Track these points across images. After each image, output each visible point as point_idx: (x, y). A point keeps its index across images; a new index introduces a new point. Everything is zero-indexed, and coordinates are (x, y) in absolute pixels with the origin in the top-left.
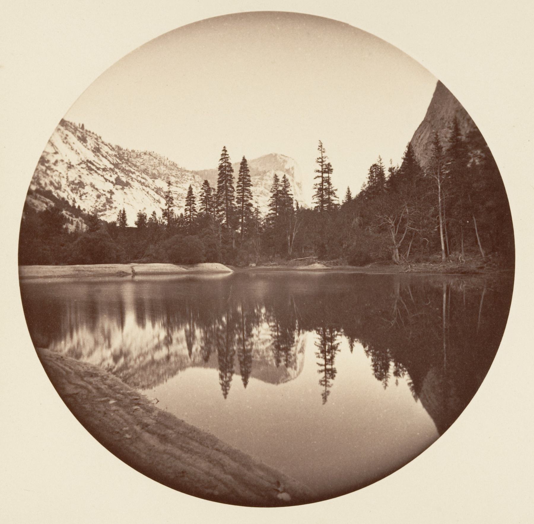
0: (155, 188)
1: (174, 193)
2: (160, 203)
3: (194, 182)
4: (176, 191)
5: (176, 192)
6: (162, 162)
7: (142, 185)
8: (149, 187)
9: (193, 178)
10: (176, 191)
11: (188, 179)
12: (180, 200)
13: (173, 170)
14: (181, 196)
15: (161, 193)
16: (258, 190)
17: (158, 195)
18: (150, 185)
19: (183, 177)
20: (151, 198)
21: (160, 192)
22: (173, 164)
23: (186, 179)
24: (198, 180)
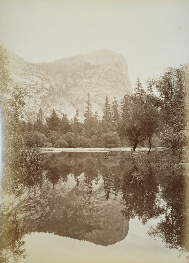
9: (38, 71)
11: (34, 72)
19: (30, 69)
23: (33, 72)
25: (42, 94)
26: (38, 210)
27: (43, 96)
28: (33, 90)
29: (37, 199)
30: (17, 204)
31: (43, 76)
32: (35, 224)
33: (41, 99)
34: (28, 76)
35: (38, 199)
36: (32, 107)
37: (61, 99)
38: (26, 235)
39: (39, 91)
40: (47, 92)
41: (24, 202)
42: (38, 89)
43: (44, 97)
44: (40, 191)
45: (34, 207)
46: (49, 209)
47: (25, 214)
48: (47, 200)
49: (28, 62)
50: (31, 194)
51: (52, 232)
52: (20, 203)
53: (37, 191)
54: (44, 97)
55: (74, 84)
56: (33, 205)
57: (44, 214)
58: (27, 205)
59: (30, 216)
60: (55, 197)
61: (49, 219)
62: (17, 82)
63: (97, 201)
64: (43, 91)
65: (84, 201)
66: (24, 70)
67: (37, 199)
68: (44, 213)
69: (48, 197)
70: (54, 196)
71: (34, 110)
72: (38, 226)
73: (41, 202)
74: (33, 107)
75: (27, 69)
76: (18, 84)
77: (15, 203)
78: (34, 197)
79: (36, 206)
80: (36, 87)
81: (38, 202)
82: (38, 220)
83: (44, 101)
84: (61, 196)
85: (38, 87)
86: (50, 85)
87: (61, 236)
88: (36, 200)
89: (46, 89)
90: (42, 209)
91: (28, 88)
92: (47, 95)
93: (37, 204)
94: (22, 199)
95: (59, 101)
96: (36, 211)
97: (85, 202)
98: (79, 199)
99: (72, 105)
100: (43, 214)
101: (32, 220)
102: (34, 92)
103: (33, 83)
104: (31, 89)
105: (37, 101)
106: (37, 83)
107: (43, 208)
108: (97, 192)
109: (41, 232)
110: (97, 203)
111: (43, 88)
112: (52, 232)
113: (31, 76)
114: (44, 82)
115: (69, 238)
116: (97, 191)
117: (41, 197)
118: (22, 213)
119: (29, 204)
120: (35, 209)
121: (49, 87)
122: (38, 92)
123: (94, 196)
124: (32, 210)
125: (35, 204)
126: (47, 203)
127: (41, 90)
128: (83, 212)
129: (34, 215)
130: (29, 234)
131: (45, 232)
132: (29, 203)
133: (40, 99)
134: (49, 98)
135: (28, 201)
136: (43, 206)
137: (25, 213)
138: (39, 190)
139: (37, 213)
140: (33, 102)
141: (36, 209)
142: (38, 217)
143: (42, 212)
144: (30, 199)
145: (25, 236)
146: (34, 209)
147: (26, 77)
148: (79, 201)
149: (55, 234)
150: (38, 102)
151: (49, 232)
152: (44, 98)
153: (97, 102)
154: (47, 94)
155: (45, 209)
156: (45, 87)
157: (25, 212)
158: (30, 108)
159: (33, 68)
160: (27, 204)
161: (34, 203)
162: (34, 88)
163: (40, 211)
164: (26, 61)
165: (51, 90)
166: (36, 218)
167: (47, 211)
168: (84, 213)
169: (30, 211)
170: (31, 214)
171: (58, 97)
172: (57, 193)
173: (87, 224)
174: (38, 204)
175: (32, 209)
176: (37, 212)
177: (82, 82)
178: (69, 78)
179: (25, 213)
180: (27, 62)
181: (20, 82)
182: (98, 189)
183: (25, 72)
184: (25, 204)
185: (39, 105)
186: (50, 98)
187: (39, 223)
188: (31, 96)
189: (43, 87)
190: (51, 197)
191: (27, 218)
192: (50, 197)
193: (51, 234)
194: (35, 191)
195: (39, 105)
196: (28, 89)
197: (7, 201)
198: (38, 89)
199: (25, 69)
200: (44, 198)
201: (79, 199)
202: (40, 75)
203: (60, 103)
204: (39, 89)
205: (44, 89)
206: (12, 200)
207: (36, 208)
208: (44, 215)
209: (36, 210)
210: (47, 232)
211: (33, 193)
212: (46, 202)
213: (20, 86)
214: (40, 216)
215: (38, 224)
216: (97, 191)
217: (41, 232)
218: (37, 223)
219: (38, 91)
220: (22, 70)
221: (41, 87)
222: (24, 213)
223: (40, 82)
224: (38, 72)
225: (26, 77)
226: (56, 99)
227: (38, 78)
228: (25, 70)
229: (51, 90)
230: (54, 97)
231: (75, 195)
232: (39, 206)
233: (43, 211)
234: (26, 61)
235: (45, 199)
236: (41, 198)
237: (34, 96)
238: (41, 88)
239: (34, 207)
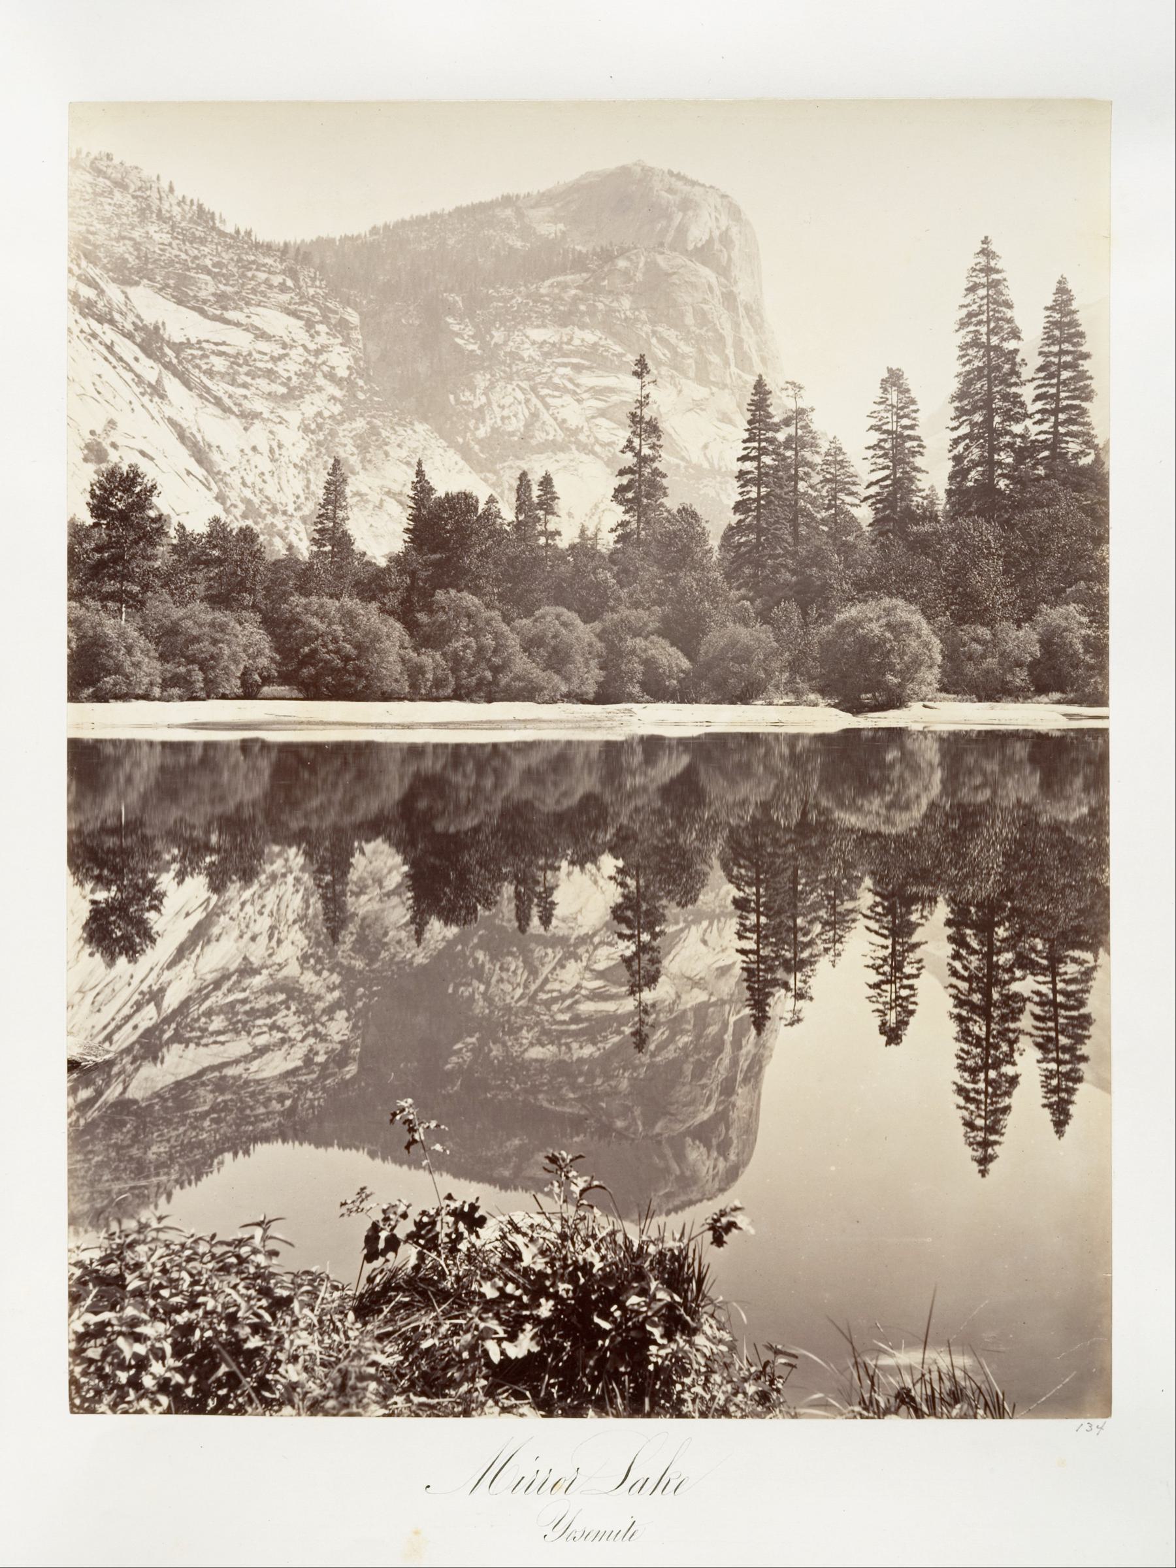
0: (137, 328)
1: (213, 352)
2: (162, 397)
3: (297, 299)
4: (224, 343)
5: (223, 348)
6: (149, 206)
7: (85, 316)
8: (112, 322)
9: (290, 283)
10: (224, 343)
11: (271, 287)
12: (245, 385)
13: (203, 242)
14: (246, 363)
15: (167, 350)
16: (576, 342)
17: (151, 362)
18: (117, 316)
19: (249, 274)
20: (129, 376)
21: (161, 349)
22: (200, 217)
23: (263, 288)
24: (311, 291)
25: (312, 404)
26: (286, 1032)
27: (320, 414)
28: (263, 383)
29: (285, 972)
30: (182, 996)
31: (315, 310)
32: (274, 1102)
33: (306, 429)
34: (235, 309)
35: (293, 969)
36: (263, 474)
37: (410, 432)
38: (228, 1156)
39: (295, 388)
40: (338, 393)
41: (217, 985)
42: (289, 379)
43: (320, 420)
44: (301, 929)
45: (270, 1011)
46: (345, 1025)
47: (222, 1048)
48: (336, 979)
49: (238, 232)
50: (253, 946)
51: (357, 1143)
52: (199, 990)
53: (283, 927)
54: (320, 420)
55: (479, 352)
56: (261, 1004)
57: (322, 1052)
58: (232, 1005)
59: (247, 1058)
60: (377, 965)
61: (348, 1077)
62: (182, 344)
63: (598, 983)
64: (320, 389)
65: (526, 987)
66: (214, 276)
67: (285, 972)
68: (321, 1047)
69: (339, 964)
70: (372, 958)
71: (271, 490)
72: (291, 1111)
73: (306, 991)
74: (267, 477)
75: (235, 270)
76: (189, 351)
77: (168, 993)
78: (269, 962)
79: (279, 1010)
80: (280, 368)
81: (291, 991)
82: (288, 1083)
83: (319, 443)
84: (409, 956)
85: (290, 368)
86: (354, 357)
87: (405, 1167)
88: (280, 976)
89: (331, 376)
90: (311, 1028)
91: (239, 373)
92: (337, 409)
93: (281, 997)
94: (211, 972)
95: (399, 446)
96: (280, 1035)
97: (533, 987)
99: (468, 468)
100: (317, 1053)
101: (257, 1082)
102: (269, 394)
103: (263, 346)
104: (253, 379)
105: (287, 443)
106: (284, 346)
107: (314, 1021)
108: (596, 940)
109: (301, 1144)
110: (595, 996)
111: (319, 374)
112: (357, 1143)
113: (253, 309)
114: (323, 339)
115: (444, 1174)
116: (594, 934)
117: (304, 958)
118: (206, 1045)
119: (241, 996)
120: (273, 1027)
121: (349, 368)
122: (293, 395)
123: (578, 958)
124: (256, 1031)
125: (273, 1000)
126: (336, 994)
127: (305, 383)
128: (521, 1045)
129: (267, 1057)
130: (240, 1154)
131: (321, 1142)
132: (244, 990)
133: (301, 433)
134: (346, 425)
135: (239, 982)
136: (313, 1011)
137: (223, 1043)
138: (296, 927)
139: (286, 1046)
140: (264, 448)
141: (279, 1023)
142: (290, 1065)
143: (311, 1041)
144: (247, 970)
145: (221, 1163)
146: (265, 1025)
147: (231, 315)
148: (501, 986)
149: (372, 1155)
150: (291, 447)
151: (343, 1146)
152: (320, 427)
153: (597, 448)
154: (338, 405)
155: (323, 1024)
156: (325, 368)
157: (221, 1038)
158: (249, 481)
159: (264, 265)
160: (230, 998)
161: (269, 991)
162: (270, 374)
163: (299, 1037)
164: (229, 229)
165: (361, 383)
166: (277, 1072)
167: (337, 1038)
168: (526, 1050)
169: (249, 1033)
170: (250, 1050)
171: (395, 420)
172: (386, 944)
173: (541, 1106)
174: (290, 997)
175: (260, 1022)
176: (283, 1041)
177: (523, 343)
178: (450, 320)
179: (223, 1043)
180: (232, 237)
181: (199, 342)
182: (598, 925)
183: (222, 287)
184: (225, 995)
185: (295, 465)
186: (354, 425)
187: (292, 1096)
188: (257, 415)
189: (314, 366)
190: (359, 964)
191: (230, 1072)
192: (353, 962)
193: (351, 1154)
194: (272, 928)
195: (295, 465)
196: (240, 381)
197: (132, 977)
198: (289, 379)
199: (224, 271)
200: (319, 967)
201: (504, 975)
202: (301, 304)
203: (404, 453)
204: (294, 378)
205: (320, 380)
206: (159, 976)
207: (279, 1019)
208: (321, 1059)
209: (279, 1029)
210: (332, 1145)
211: (263, 940)
212: (331, 989)
213: (198, 361)
214: (299, 1063)
215: (288, 1103)
216: (594, 934)
217: (301, 1144)
218: (281, 1098)
219: (291, 390)
220: (208, 278)
221: (304, 369)
222: (215, 1042)
223: (301, 342)
224: (290, 288)
225: (231, 315)
226: (384, 433)
227: (292, 321)
228: (223, 275)
229: (361, 383)
230: (377, 422)
231: (480, 955)
232: (293, 1008)
233: (316, 1034)
234: (228, 231)
235: (325, 973)
236: (308, 969)
237: (272, 417)
238: (304, 375)
239: (270, 1011)
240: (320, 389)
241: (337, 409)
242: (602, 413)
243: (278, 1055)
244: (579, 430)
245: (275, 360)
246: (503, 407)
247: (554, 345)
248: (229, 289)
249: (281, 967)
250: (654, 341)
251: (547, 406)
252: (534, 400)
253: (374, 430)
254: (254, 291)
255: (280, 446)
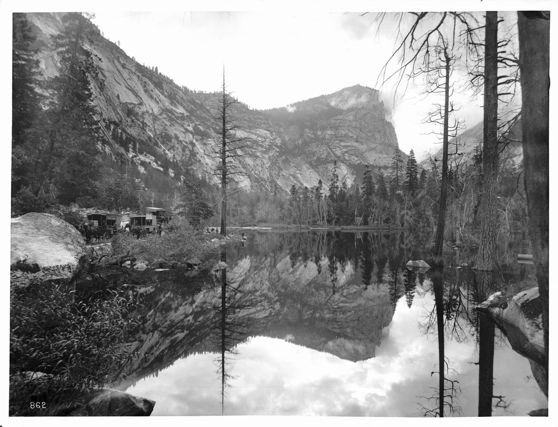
11: (261, 123)
16: (340, 134)
40: (278, 150)
59: (255, 313)
64: (274, 149)
85: (267, 144)
89: (276, 146)
98: (320, 295)
105: (265, 163)
120: (261, 305)
126: (277, 298)
156: (275, 144)
161: (261, 296)
162: (262, 146)
167: (277, 309)
205: (274, 147)
207: (263, 303)
209: (263, 306)
212: (275, 297)
218: (263, 323)
233: (272, 308)
239: (261, 301)
240: (274, 149)
241: (277, 154)
242: (346, 152)
243: (263, 312)
244: (340, 157)
245: (262, 142)
246: (320, 152)
247: (334, 135)
248: (251, 124)
249: (263, 290)
250: (361, 132)
251: (332, 151)
252: (328, 149)
253: (287, 159)
254: (257, 125)
255: (264, 164)
